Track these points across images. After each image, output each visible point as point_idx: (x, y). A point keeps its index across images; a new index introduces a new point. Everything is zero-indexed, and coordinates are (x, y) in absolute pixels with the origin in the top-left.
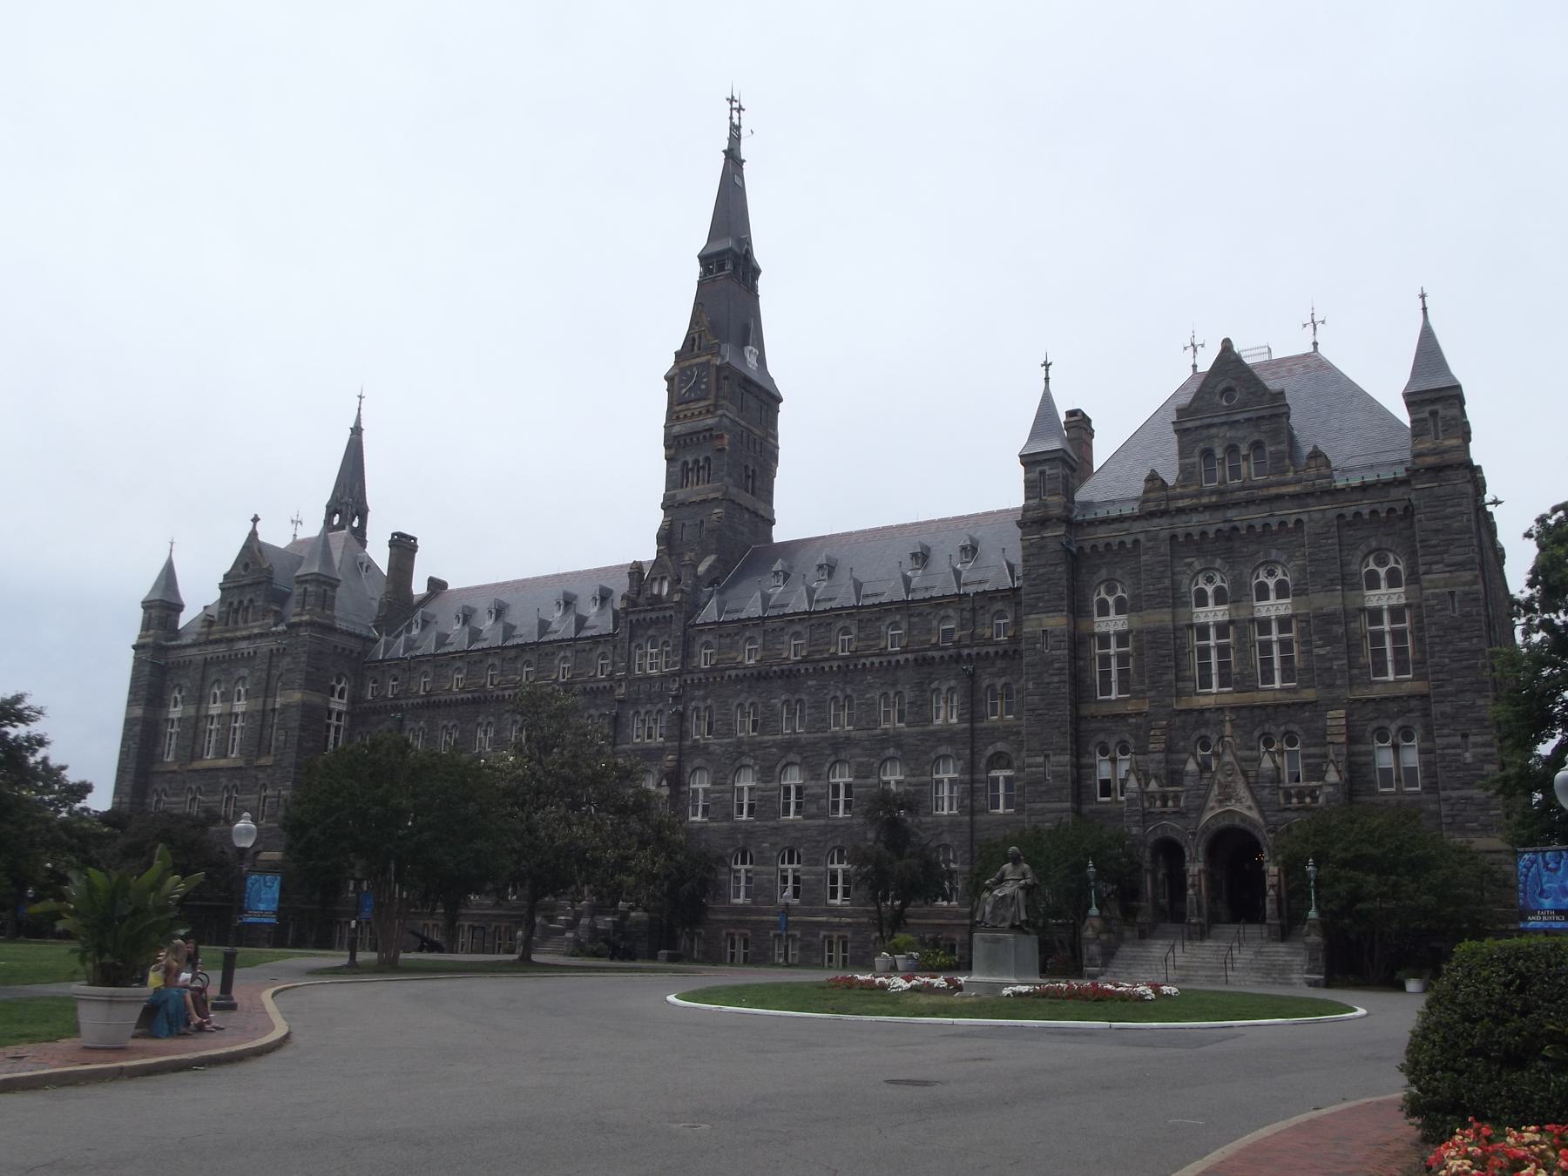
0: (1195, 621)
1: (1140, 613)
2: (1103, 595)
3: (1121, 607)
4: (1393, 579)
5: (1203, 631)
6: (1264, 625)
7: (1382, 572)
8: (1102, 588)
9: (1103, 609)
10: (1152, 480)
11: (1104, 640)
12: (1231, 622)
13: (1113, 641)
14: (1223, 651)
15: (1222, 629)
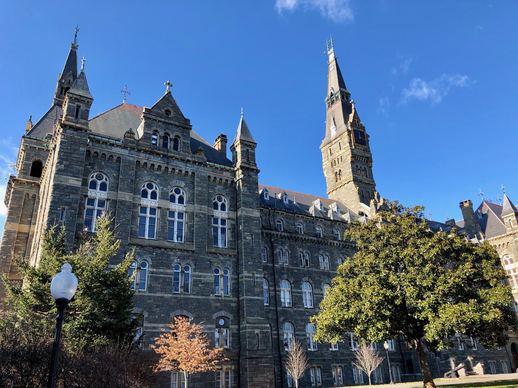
0: (142, 203)
1: (115, 192)
2: (94, 178)
3: (103, 187)
4: (223, 208)
5: (144, 209)
6: (172, 214)
7: (220, 204)
8: (95, 174)
9: (93, 185)
10: (131, 133)
11: (91, 201)
12: (159, 208)
13: (96, 203)
14: (152, 220)
15: (153, 211)
